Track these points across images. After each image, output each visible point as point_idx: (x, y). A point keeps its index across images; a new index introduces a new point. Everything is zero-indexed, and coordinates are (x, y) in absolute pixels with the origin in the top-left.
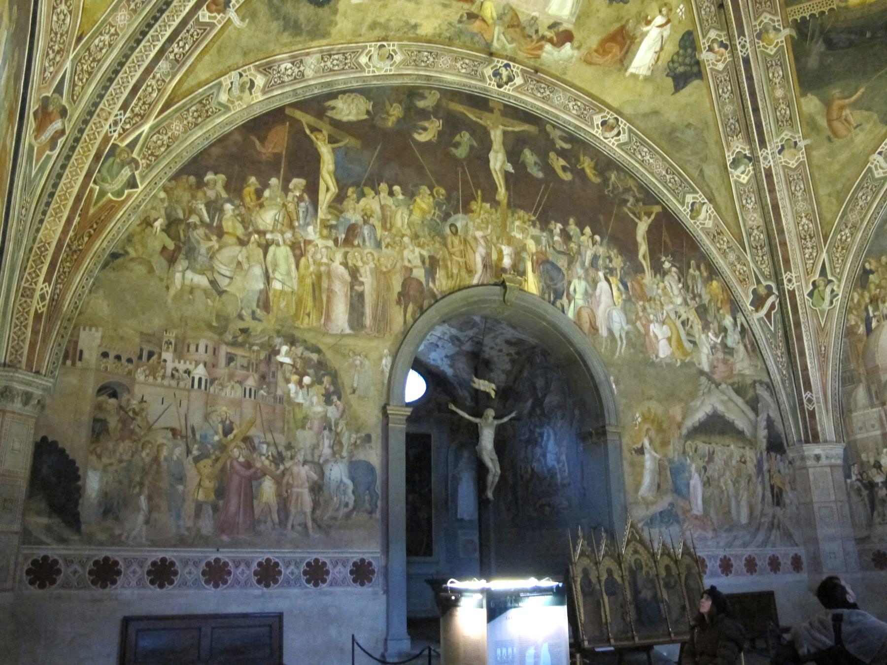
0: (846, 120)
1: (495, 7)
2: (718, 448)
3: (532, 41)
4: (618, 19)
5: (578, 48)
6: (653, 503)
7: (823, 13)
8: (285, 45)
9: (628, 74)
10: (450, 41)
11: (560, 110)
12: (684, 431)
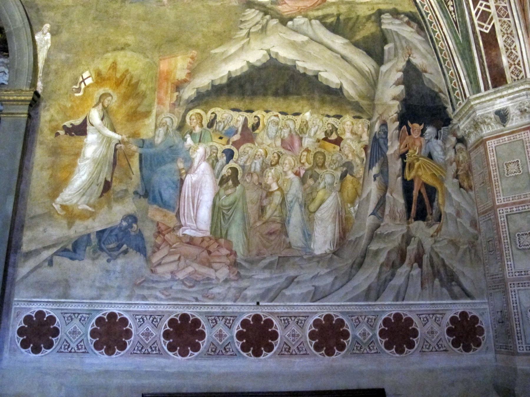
2: (265, 118)
6: (84, 216)
12: (189, 93)
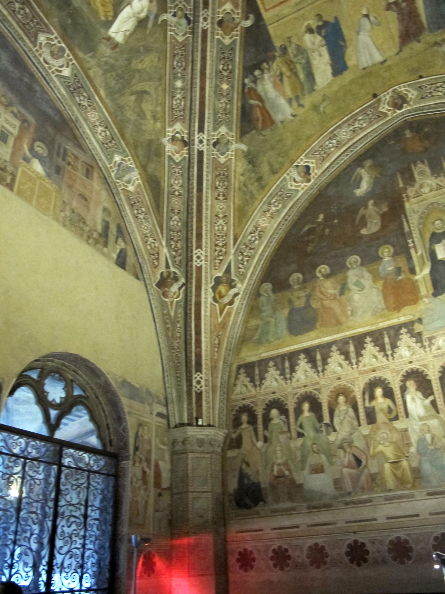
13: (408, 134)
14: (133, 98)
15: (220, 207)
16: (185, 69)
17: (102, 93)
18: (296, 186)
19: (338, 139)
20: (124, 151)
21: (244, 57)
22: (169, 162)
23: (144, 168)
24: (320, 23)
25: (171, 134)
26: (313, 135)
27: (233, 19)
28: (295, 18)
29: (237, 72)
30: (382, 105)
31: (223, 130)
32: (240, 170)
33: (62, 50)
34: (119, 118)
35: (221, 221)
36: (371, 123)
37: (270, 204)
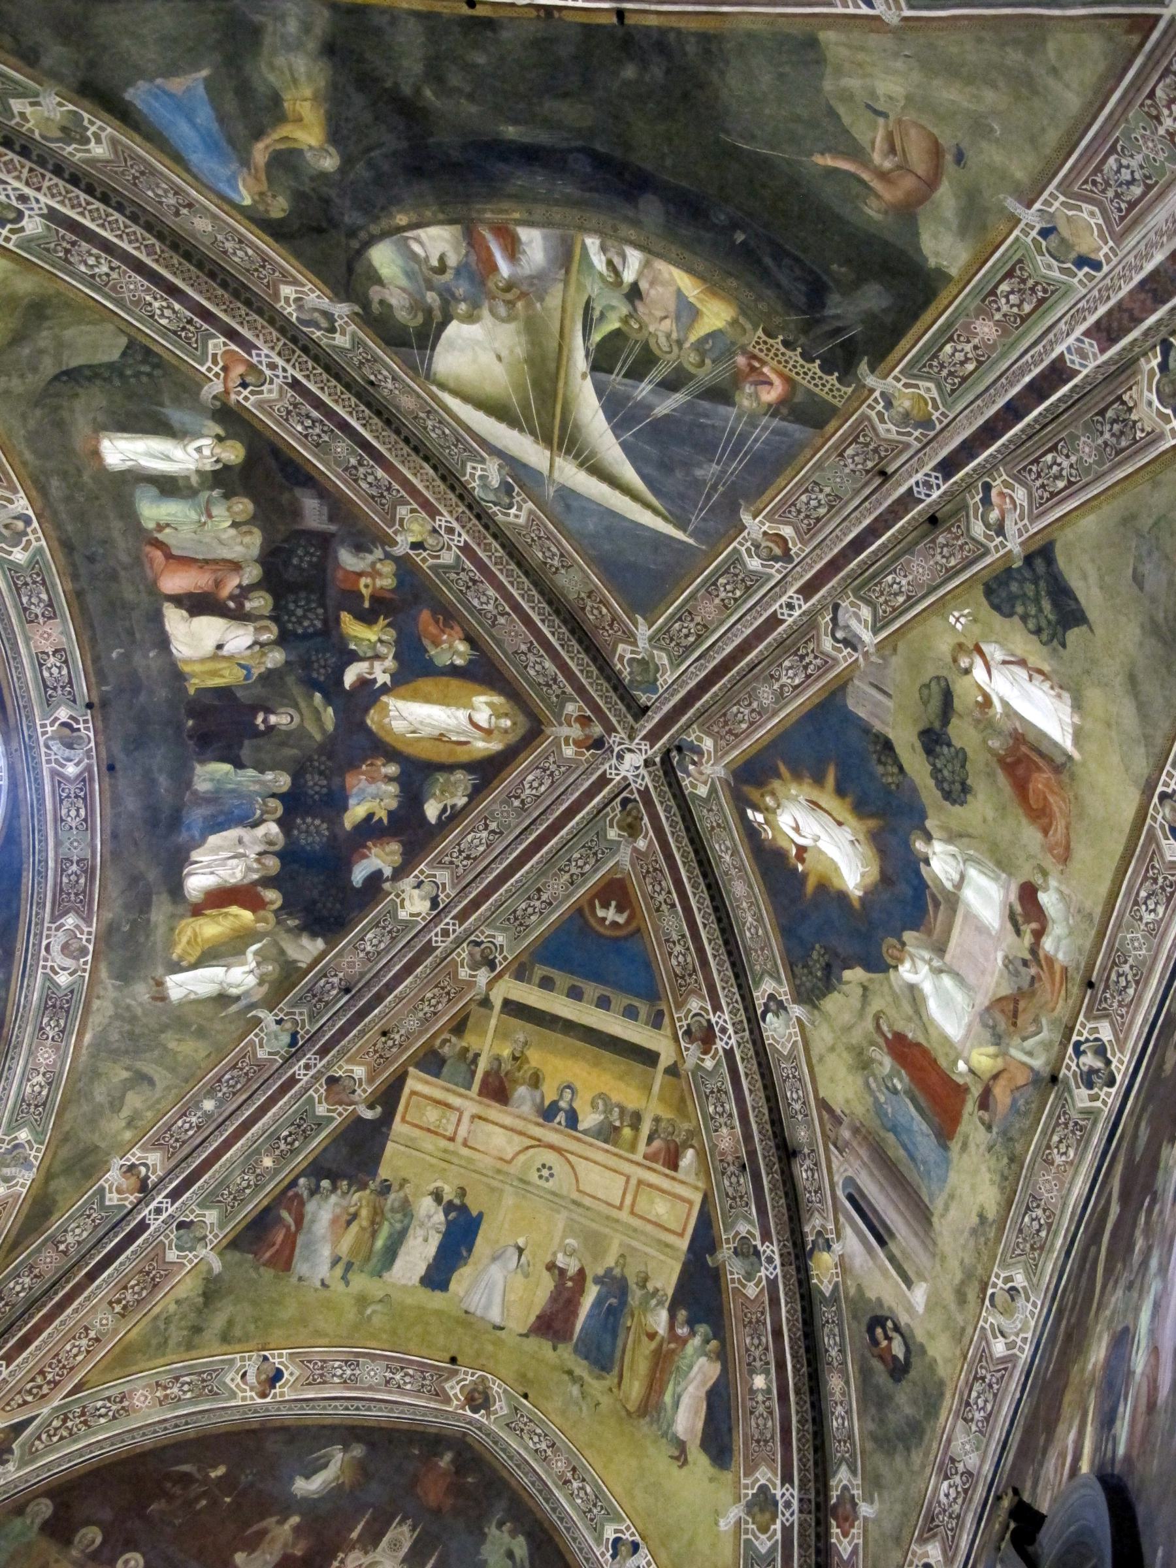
0: (892, 150)
1: (981, 1045)
3: (1040, 979)
4: (991, 775)
5: (1045, 873)
7: (786, 344)
8: (923, 1466)
9: (1076, 756)
10: (1015, 1159)
11: (1160, 945)
13: (445, 1461)
14: (125, 1074)
15: (103, 1320)
16: (234, 1094)
17: (88, 1038)
18: (237, 1386)
19: (357, 1372)
20: (44, 1132)
21: (325, 1150)
22: (94, 1194)
23: (49, 1176)
24: (457, 1201)
25: (133, 1160)
26: (326, 1335)
27: (354, 1092)
28: (431, 1165)
29: (300, 1160)
30: (453, 1382)
31: (211, 1216)
32: (182, 1292)
33: (83, 951)
34: (81, 1085)
35: (84, 1342)
36: (418, 1392)
37: (177, 1379)
